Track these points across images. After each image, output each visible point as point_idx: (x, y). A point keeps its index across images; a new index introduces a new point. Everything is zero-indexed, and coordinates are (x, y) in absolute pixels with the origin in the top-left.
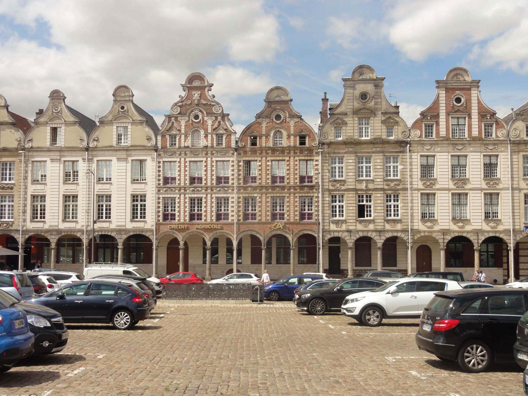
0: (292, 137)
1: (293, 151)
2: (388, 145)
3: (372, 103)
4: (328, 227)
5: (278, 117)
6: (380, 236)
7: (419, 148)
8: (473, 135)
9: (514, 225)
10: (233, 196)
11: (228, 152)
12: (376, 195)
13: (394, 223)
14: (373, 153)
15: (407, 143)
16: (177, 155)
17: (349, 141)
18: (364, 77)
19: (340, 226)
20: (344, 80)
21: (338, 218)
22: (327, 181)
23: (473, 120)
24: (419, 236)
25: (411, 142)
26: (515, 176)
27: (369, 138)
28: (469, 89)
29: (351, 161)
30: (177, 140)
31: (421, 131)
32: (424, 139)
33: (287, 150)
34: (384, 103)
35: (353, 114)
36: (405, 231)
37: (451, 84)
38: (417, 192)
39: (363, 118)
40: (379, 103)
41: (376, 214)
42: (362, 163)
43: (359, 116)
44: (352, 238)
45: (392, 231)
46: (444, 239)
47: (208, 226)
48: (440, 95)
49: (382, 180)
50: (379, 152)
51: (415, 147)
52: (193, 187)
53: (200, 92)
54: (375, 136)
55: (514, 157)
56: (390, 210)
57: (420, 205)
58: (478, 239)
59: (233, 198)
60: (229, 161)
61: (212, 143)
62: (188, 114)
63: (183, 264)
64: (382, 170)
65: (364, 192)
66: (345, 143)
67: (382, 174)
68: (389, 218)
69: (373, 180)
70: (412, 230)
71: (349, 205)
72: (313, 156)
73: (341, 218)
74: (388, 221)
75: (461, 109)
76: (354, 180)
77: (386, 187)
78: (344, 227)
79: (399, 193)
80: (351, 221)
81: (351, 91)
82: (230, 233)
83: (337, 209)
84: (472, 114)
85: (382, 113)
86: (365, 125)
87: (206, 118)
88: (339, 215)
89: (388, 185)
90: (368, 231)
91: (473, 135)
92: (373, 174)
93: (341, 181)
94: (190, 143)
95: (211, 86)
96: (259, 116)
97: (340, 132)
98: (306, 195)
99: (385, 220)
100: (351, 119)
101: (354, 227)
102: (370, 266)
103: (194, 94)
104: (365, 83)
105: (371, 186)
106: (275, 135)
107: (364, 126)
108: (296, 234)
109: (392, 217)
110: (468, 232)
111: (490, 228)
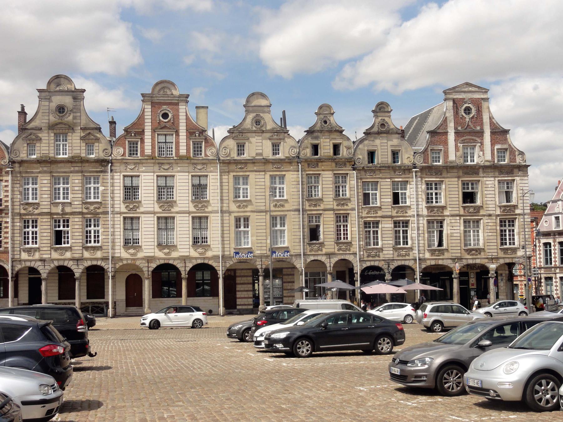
2: (87, 164)
3: (71, 118)
4: (18, 256)
6: (78, 265)
7: (123, 167)
8: (180, 154)
9: (223, 251)
12: (73, 220)
13: (93, 250)
14: (71, 172)
15: (107, 162)
17: (44, 159)
18: (61, 88)
19: (32, 254)
20: (40, 91)
21: (30, 245)
22: (18, 204)
23: (181, 137)
24: (121, 264)
25: (113, 161)
26: (224, 198)
27: (66, 156)
28: (177, 104)
29: (45, 182)
31: (125, 149)
32: (127, 157)
34: (83, 118)
35: (49, 129)
36: (105, 259)
37: (158, 98)
38: (119, 216)
39: (60, 134)
40: (78, 118)
41: (74, 241)
42: (59, 184)
43: (55, 131)
44: (46, 268)
45: (91, 259)
46: (148, 267)
48: (146, 110)
49: (81, 203)
50: (77, 172)
51: (117, 167)
54: (73, 154)
55: (224, 177)
56: (90, 236)
57: (122, 230)
58: (185, 267)
64: (80, 192)
65: (61, 217)
66: (39, 162)
67: (80, 196)
68: (89, 245)
69: (70, 203)
70: (113, 257)
71: (43, 231)
72: (2, 176)
73: (34, 246)
74: (87, 248)
75: (168, 125)
76: (49, 203)
77: (85, 211)
78: (37, 256)
79: (100, 217)
80: (78, 248)
81: (47, 103)
83: (30, 236)
84: (180, 131)
85: (81, 129)
86: (63, 141)
88: (33, 242)
89: (87, 208)
90: (64, 260)
91: (180, 154)
97: (35, 150)
99: (83, 248)
100: (47, 135)
101: (49, 256)
104: (62, 95)
105: (68, 210)
107: (61, 143)
109: (93, 244)
110: (174, 259)
111: (198, 254)
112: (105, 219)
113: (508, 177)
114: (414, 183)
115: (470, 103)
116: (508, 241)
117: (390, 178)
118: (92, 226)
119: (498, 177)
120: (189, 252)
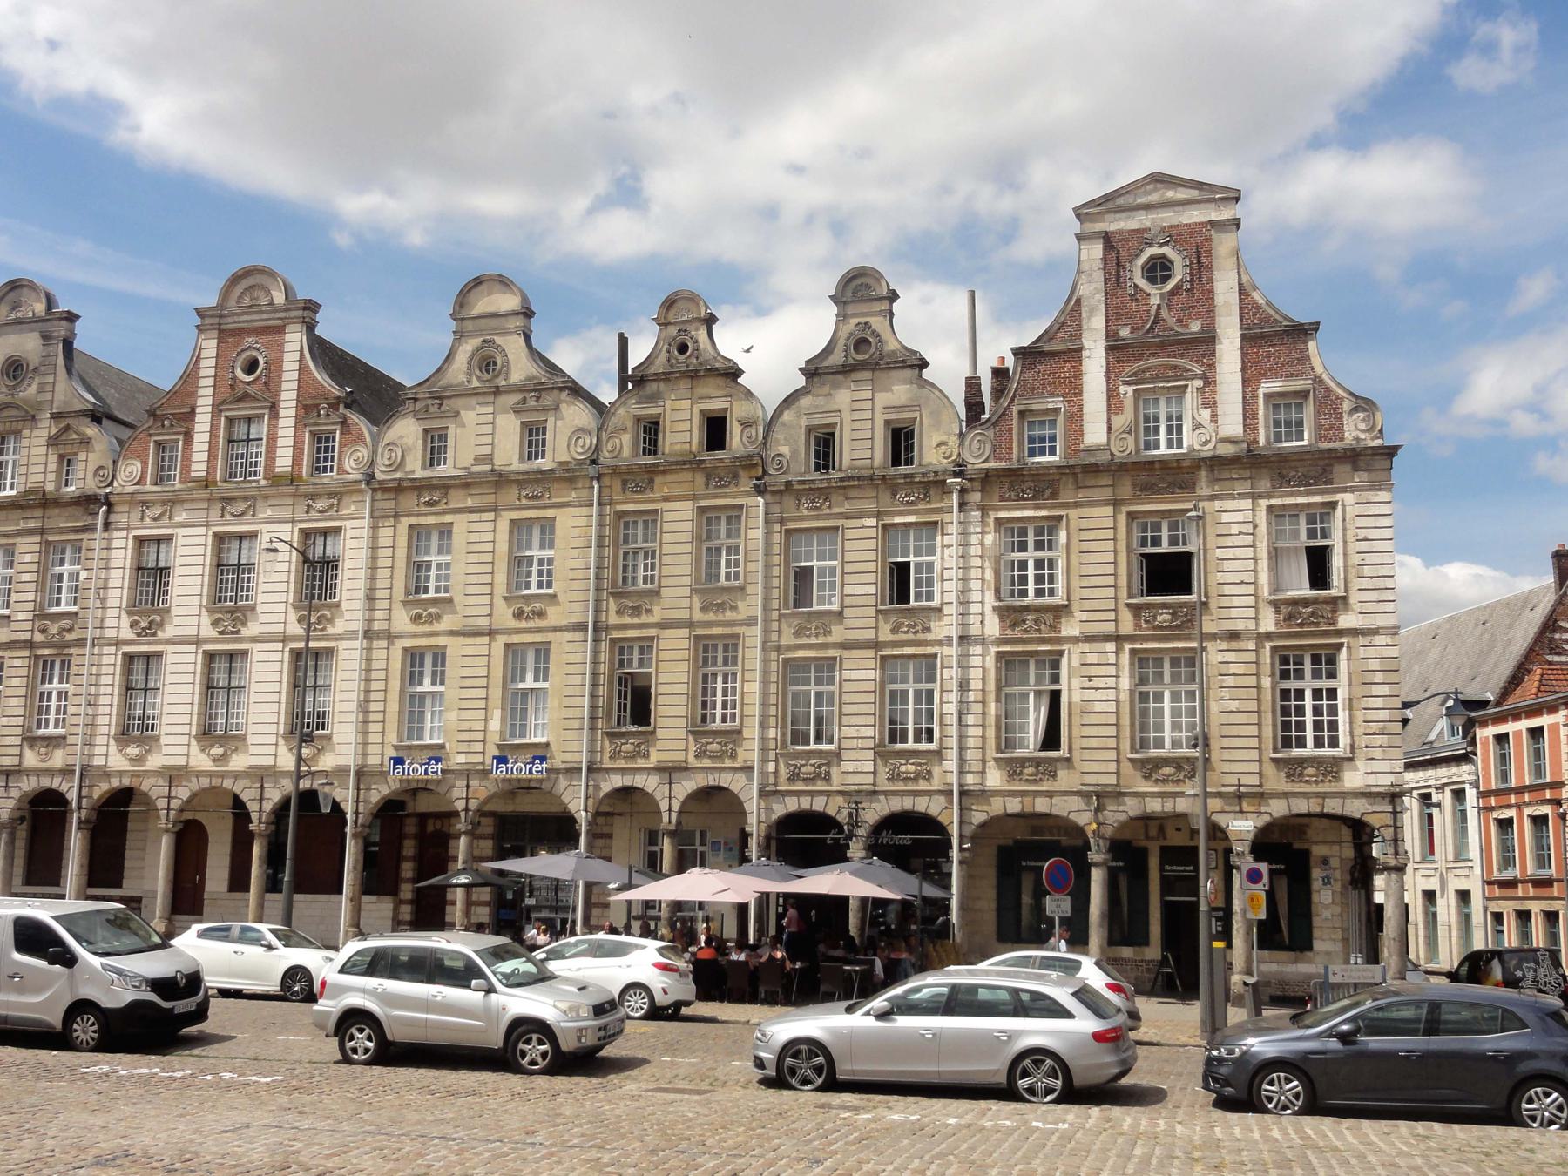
2: (57, 511)
3: (33, 389)
6: (7, 787)
18: (19, 315)
23: (281, 423)
25: (113, 499)
26: (379, 594)
28: (280, 330)
31: (144, 463)
32: (149, 487)
36: (66, 772)
37: (236, 319)
45: (39, 772)
46: (169, 797)
48: (204, 354)
50: (31, 532)
55: (382, 532)
58: (262, 799)
69: (9, 617)
74: (30, 740)
75: (251, 390)
77: (39, 637)
84: (282, 404)
89: (43, 631)
91: (277, 470)
104: (21, 331)
110: (236, 776)
113: (1308, 493)
114: (953, 529)
115: (1167, 243)
116: (1309, 734)
117: (878, 515)
118: (56, 680)
119: (1270, 496)
120: (275, 755)
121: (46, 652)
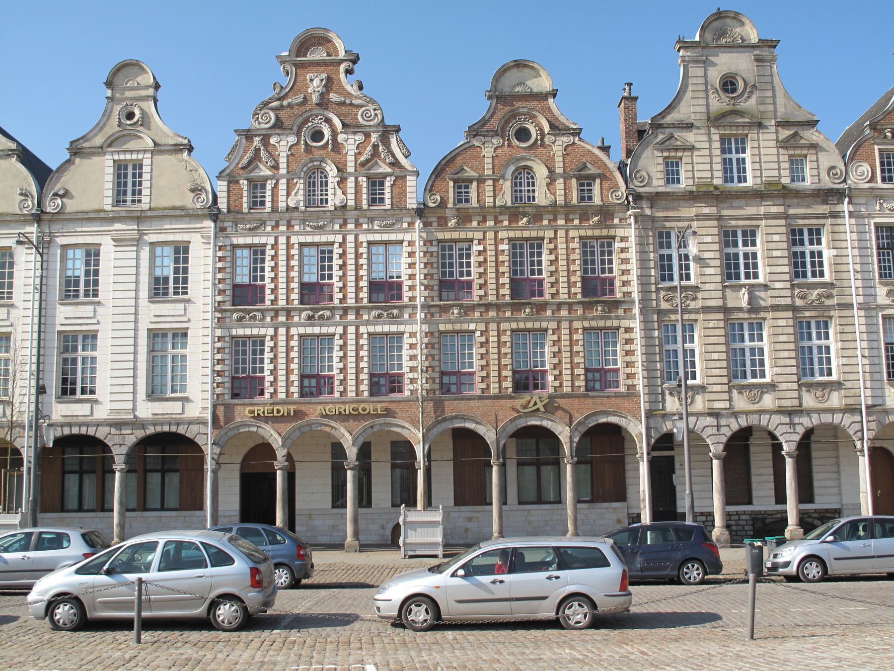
0: (560, 182)
1: (563, 216)
5: (523, 135)
10: (416, 328)
11: (400, 220)
16: (269, 229)
17: (704, 189)
30: (268, 193)
32: (879, 184)
33: (549, 213)
45: (819, 411)
47: (348, 408)
52: (311, 309)
53: (324, 76)
59: (412, 335)
60: (401, 242)
61: (357, 199)
62: (295, 129)
63: (284, 509)
65: (746, 316)
66: (692, 197)
68: (809, 379)
72: (615, 227)
77: (799, 302)
82: (407, 425)
87: (341, 138)
89: (803, 297)
90: (761, 412)
92: (765, 270)
93: (684, 289)
94: (302, 198)
95: (355, 62)
96: (475, 131)
98: (601, 324)
101: (727, 405)
102: (750, 502)
103: (312, 80)
106: (516, 178)
107: (734, 156)
108: (579, 423)
112: (844, 321)
121: (807, 314)
